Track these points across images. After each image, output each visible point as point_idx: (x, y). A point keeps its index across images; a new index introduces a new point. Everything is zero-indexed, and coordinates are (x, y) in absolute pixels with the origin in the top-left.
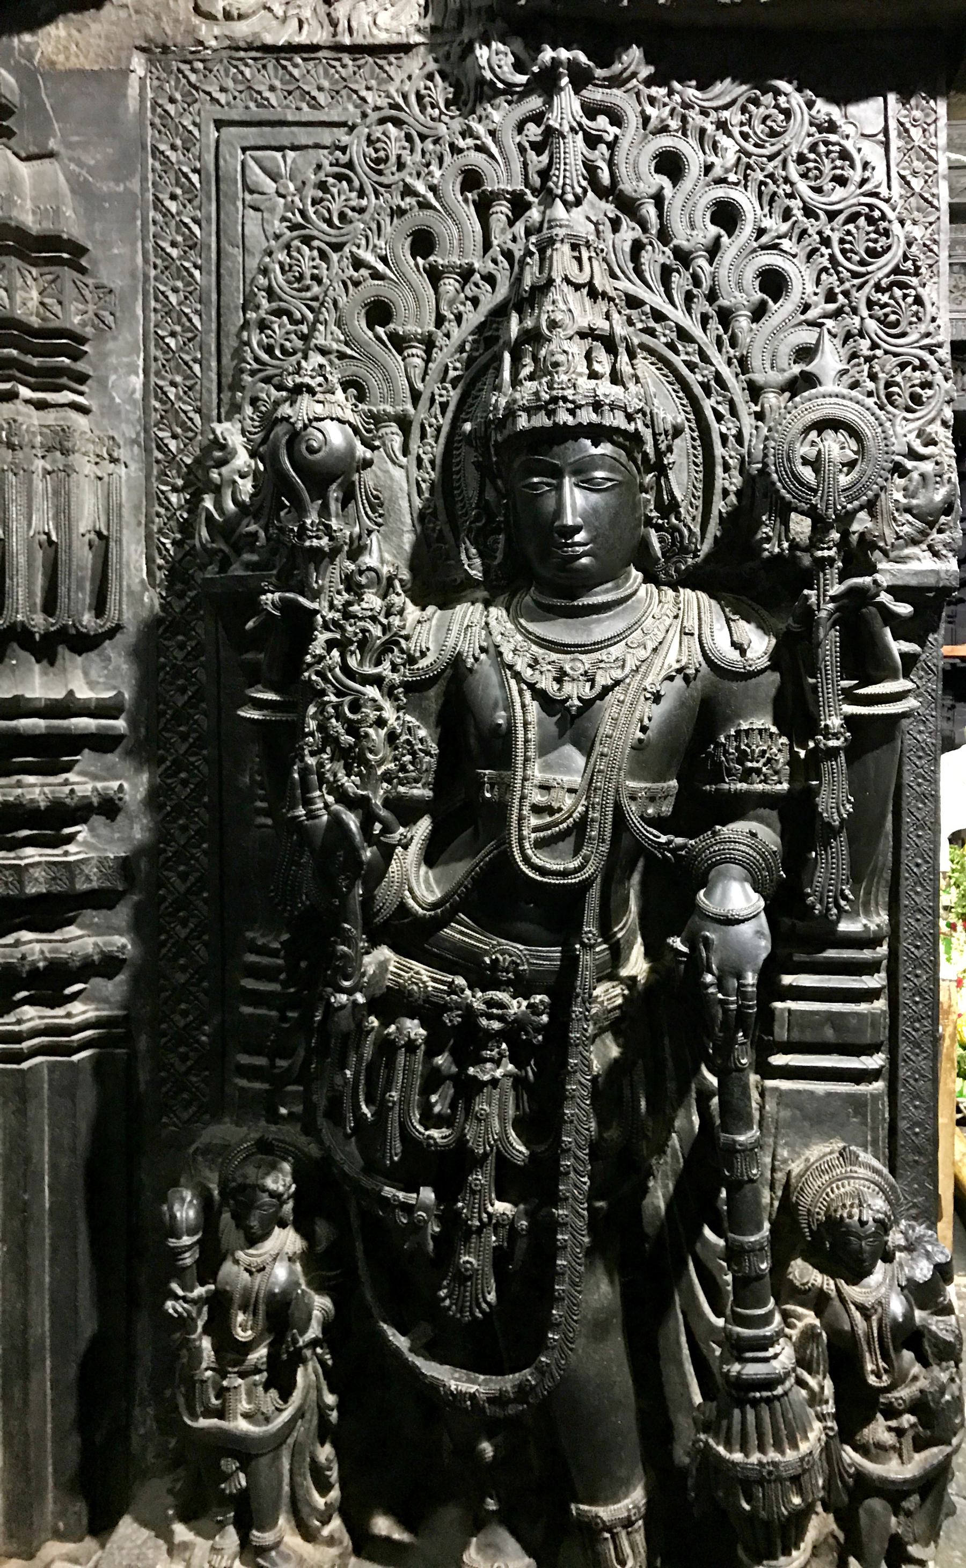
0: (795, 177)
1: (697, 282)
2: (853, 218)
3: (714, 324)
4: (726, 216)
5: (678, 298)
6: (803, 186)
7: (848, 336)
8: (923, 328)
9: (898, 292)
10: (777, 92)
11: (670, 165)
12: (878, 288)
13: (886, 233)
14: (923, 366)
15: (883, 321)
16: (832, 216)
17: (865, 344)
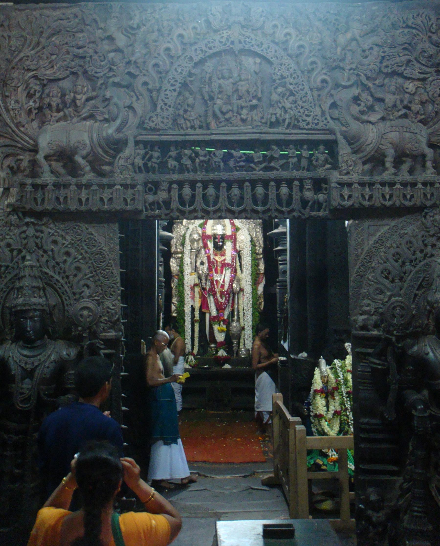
0: (84, 245)
1: (61, 269)
2: (97, 254)
3: (65, 279)
4: (68, 254)
5: (57, 273)
6: (85, 247)
7: (95, 282)
8: (113, 279)
9: (107, 271)
10: (79, 226)
11: (55, 242)
12: (102, 270)
13: (104, 257)
14: (113, 287)
15: (104, 277)
16: (92, 254)
17: (99, 283)
